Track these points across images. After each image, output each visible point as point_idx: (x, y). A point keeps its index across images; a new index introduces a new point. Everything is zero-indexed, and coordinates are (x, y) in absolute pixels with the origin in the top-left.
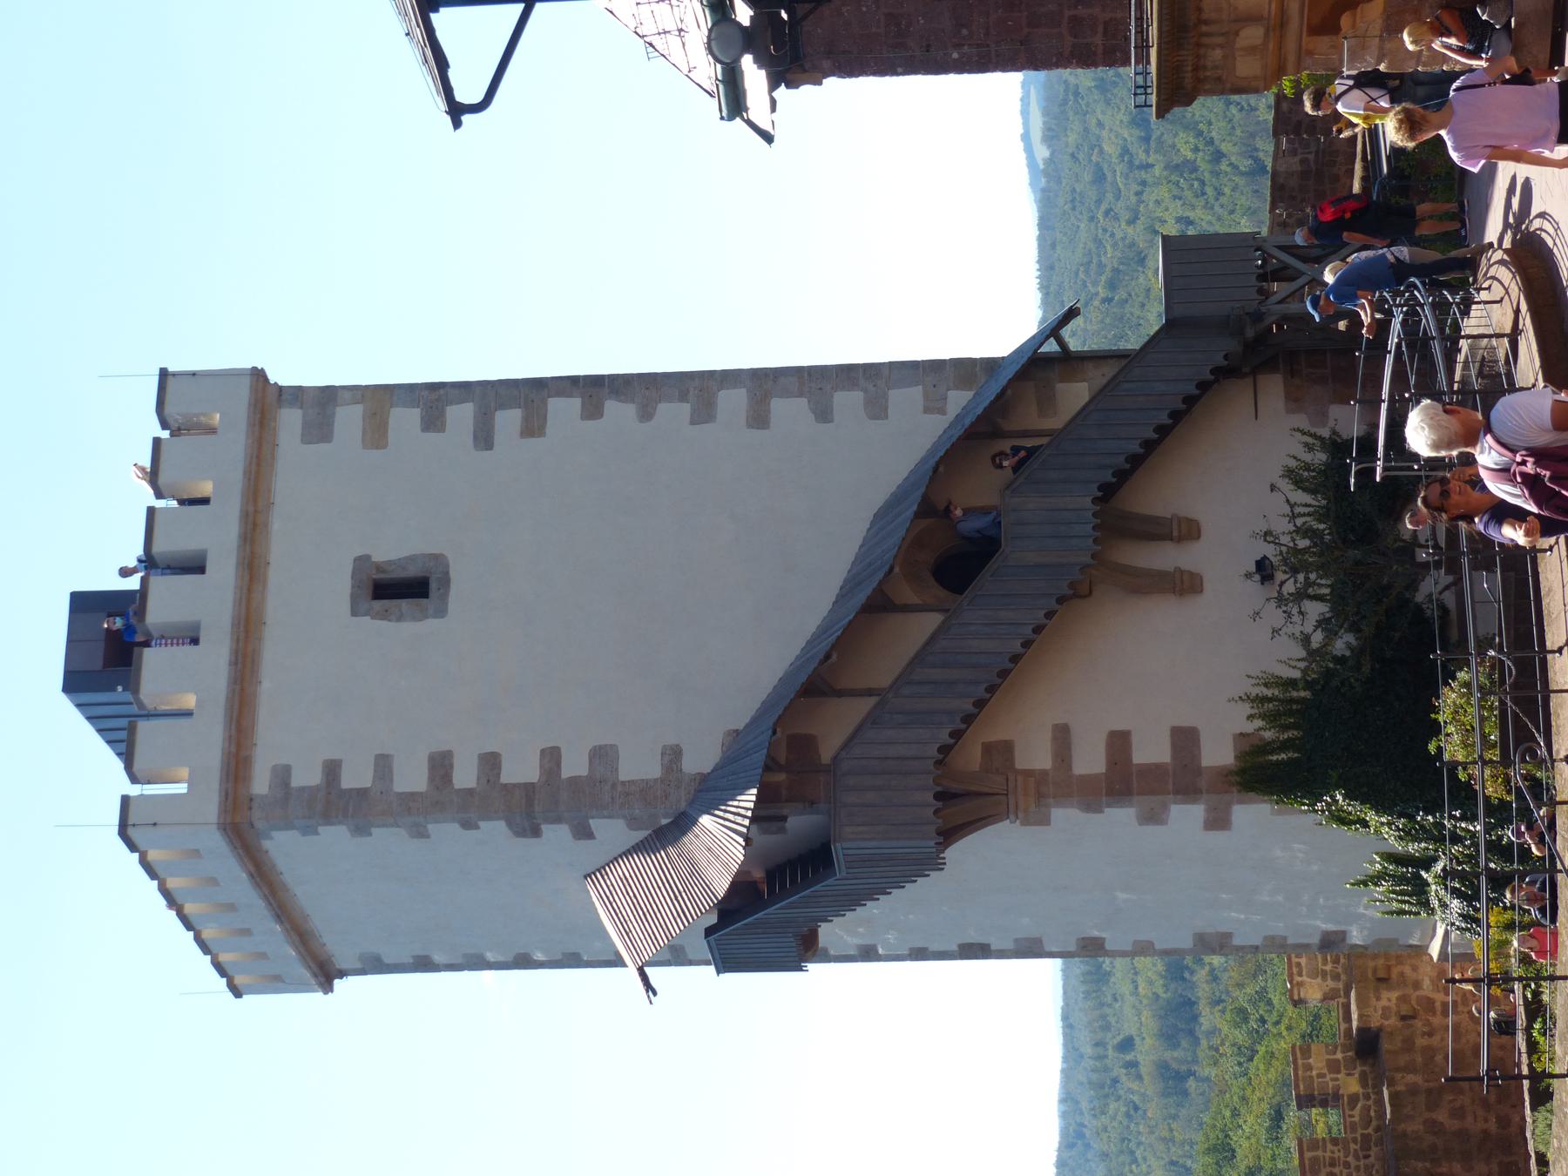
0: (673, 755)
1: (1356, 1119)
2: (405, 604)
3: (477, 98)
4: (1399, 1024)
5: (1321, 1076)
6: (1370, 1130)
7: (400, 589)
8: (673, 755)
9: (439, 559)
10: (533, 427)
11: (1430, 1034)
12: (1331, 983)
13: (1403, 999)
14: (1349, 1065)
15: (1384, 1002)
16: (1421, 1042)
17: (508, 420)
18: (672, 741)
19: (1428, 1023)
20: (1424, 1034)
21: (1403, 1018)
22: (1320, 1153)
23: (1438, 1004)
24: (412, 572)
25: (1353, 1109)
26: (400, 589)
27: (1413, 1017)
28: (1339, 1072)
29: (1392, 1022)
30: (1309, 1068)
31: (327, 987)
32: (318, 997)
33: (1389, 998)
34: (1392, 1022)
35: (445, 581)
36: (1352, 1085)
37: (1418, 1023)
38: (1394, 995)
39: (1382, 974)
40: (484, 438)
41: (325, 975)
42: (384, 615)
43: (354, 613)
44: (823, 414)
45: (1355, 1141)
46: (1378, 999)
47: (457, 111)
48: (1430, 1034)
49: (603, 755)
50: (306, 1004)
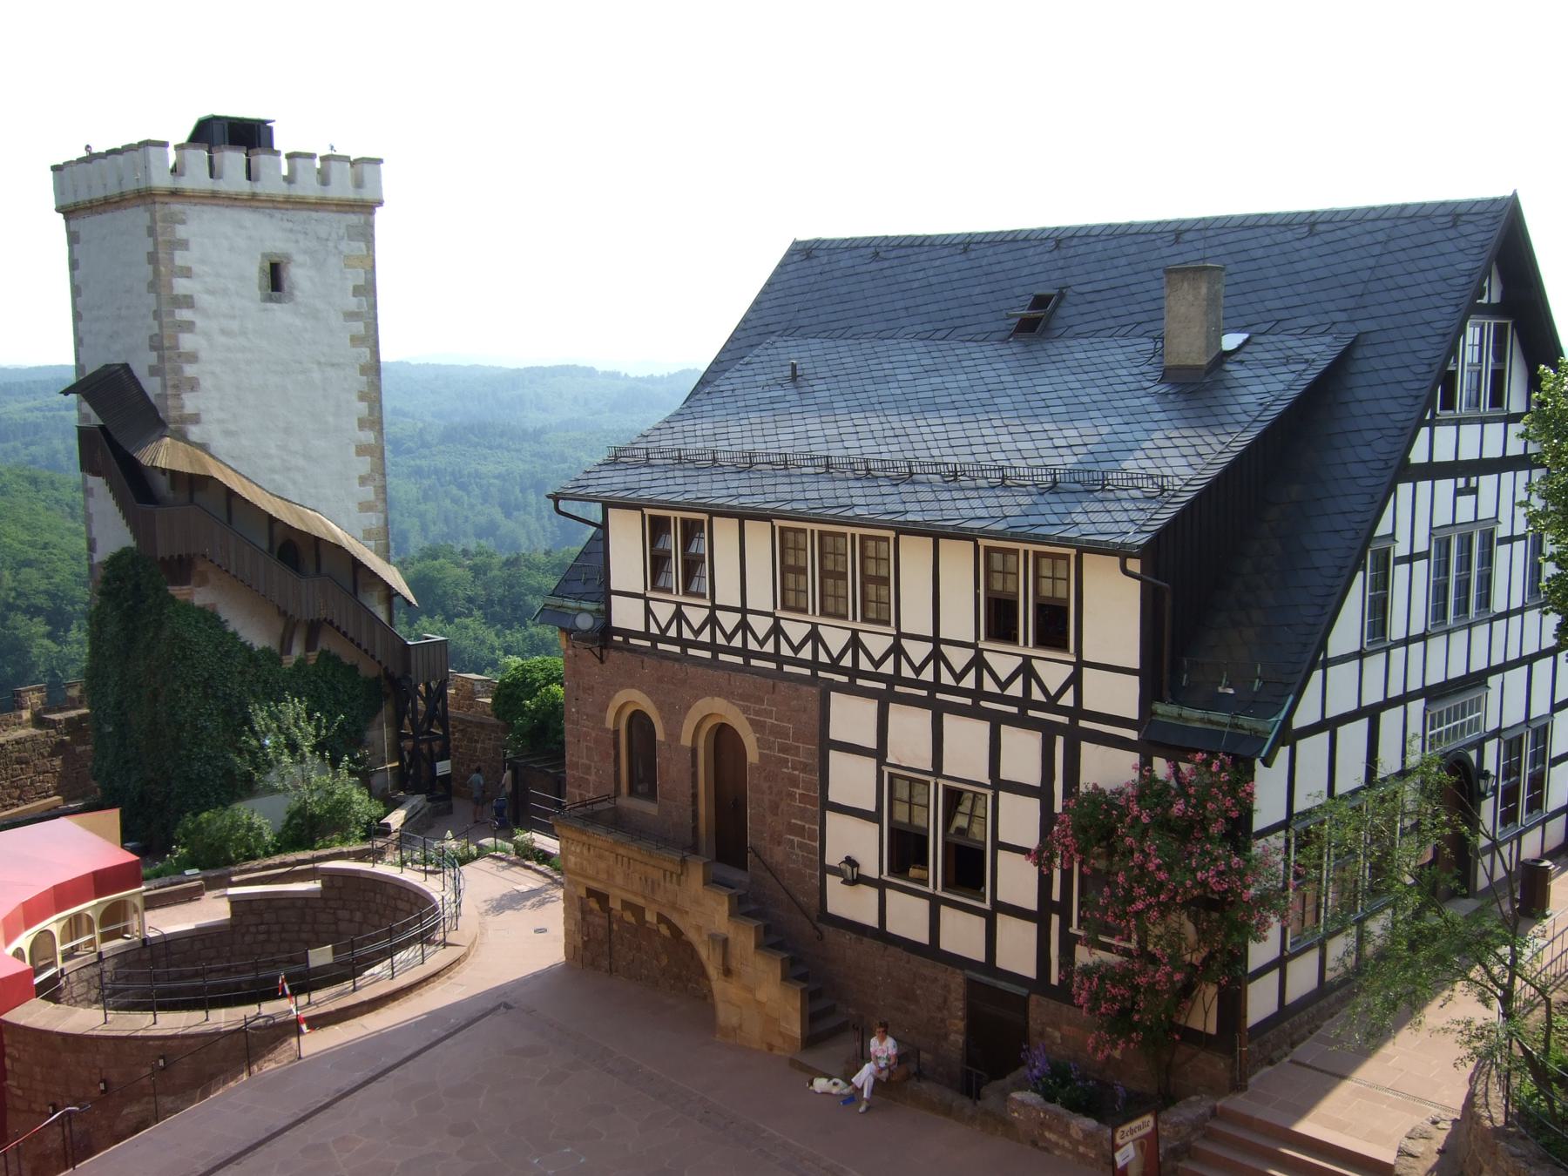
0: (195, 419)
2: (267, 281)
3: (562, 508)
7: (275, 278)
8: (195, 419)
9: (291, 297)
10: (356, 340)
17: (359, 327)
18: (204, 417)
24: (286, 285)
26: (275, 278)
31: (58, 210)
32: (54, 206)
35: (278, 301)
40: (351, 316)
41: (69, 211)
42: (262, 269)
43: (264, 255)
44: (363, 481)
47: (556, 498)
49: (193, 385)
50: (49, 199)
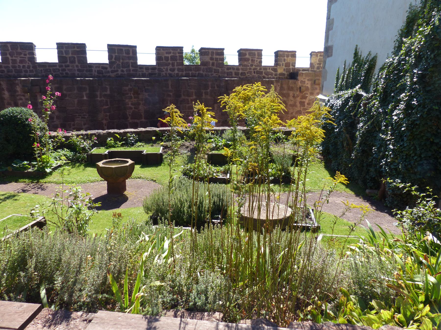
1: (268, 70)
4: (298, 86)
5: (285, 60)
6: (264, 75)
11: (294, 97)
12: (317, 66)
13: (307, 89)
14: (288, 70)
15: (307, 82)
16: (291, 93)
19: (298, 96)
20: (294, 95)
21: (300, 88)
22: (257, 56)
23: (304, 100)
25: (272, 69)
27: (300, 91)
28: (285, 66)
29: (299, 84)
30: (288, 56)
33: (308, 84)
34: (299, 84)
36: (280, 70)
37: (298, 93)
38: (309, 86)
39: (317, 82)
45: (260, 69)
46: (308, 80)
48: (294, 97)
